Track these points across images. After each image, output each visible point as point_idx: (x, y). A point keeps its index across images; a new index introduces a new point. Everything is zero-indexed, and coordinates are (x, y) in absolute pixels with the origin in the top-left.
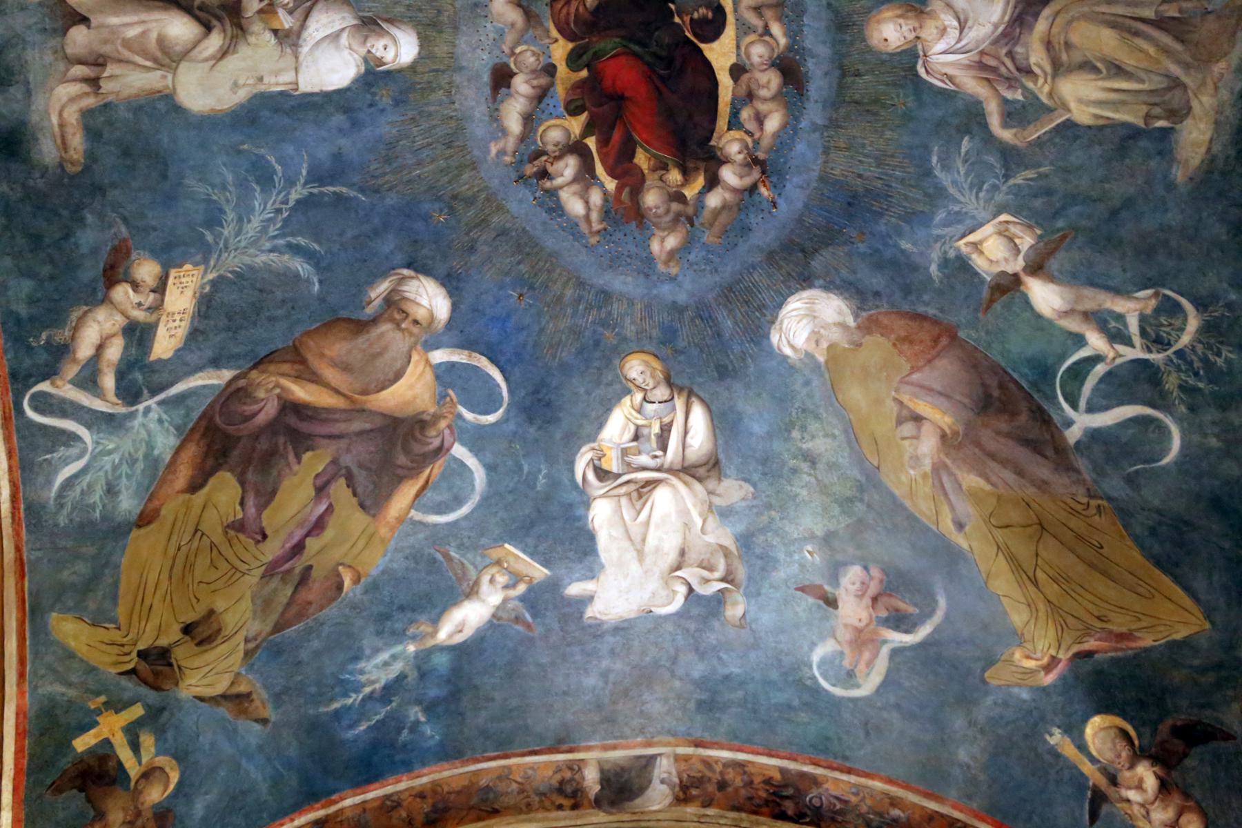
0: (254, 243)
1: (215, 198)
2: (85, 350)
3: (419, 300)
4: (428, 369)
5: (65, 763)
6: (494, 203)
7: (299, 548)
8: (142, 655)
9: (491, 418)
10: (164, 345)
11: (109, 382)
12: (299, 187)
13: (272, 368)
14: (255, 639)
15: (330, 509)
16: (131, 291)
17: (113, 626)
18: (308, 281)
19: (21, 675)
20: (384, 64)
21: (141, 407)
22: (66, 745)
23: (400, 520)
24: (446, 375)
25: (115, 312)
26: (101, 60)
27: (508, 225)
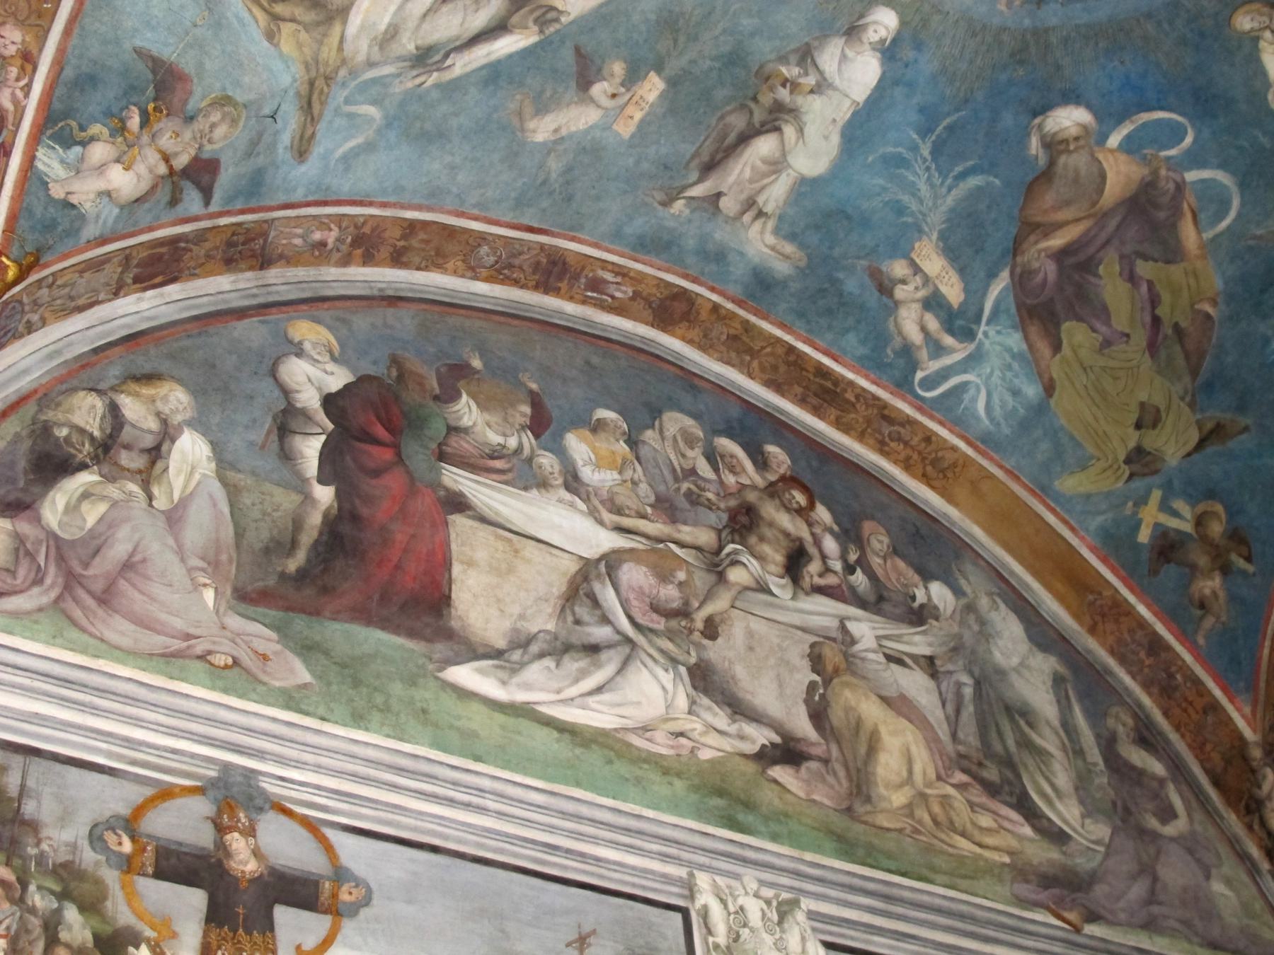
0: (936, 197)
1: (887, 199)
2: (915, 336)
3: (1063, 126)
4: (1118, 155)
5: (1145, 556)
6: (1040, 34)
7: (1156, 321)
8: (1128, 461)
9: (1189, 140)
10: (953, 292)
11: (948, 340)
12: (922, 146)
13: (1025, 246)
14: (1186, 392)
15: (1150, 284)
16: (905, 287)
18: (988, 184)
19: (1072, 529)
20: (886, 40)
21: (980, 335)
22: (1136, 547)
23: (1202, 246)
24: (1129, 147)
25: (909, 305)
26: (751, 202)
27: (1065, 33)
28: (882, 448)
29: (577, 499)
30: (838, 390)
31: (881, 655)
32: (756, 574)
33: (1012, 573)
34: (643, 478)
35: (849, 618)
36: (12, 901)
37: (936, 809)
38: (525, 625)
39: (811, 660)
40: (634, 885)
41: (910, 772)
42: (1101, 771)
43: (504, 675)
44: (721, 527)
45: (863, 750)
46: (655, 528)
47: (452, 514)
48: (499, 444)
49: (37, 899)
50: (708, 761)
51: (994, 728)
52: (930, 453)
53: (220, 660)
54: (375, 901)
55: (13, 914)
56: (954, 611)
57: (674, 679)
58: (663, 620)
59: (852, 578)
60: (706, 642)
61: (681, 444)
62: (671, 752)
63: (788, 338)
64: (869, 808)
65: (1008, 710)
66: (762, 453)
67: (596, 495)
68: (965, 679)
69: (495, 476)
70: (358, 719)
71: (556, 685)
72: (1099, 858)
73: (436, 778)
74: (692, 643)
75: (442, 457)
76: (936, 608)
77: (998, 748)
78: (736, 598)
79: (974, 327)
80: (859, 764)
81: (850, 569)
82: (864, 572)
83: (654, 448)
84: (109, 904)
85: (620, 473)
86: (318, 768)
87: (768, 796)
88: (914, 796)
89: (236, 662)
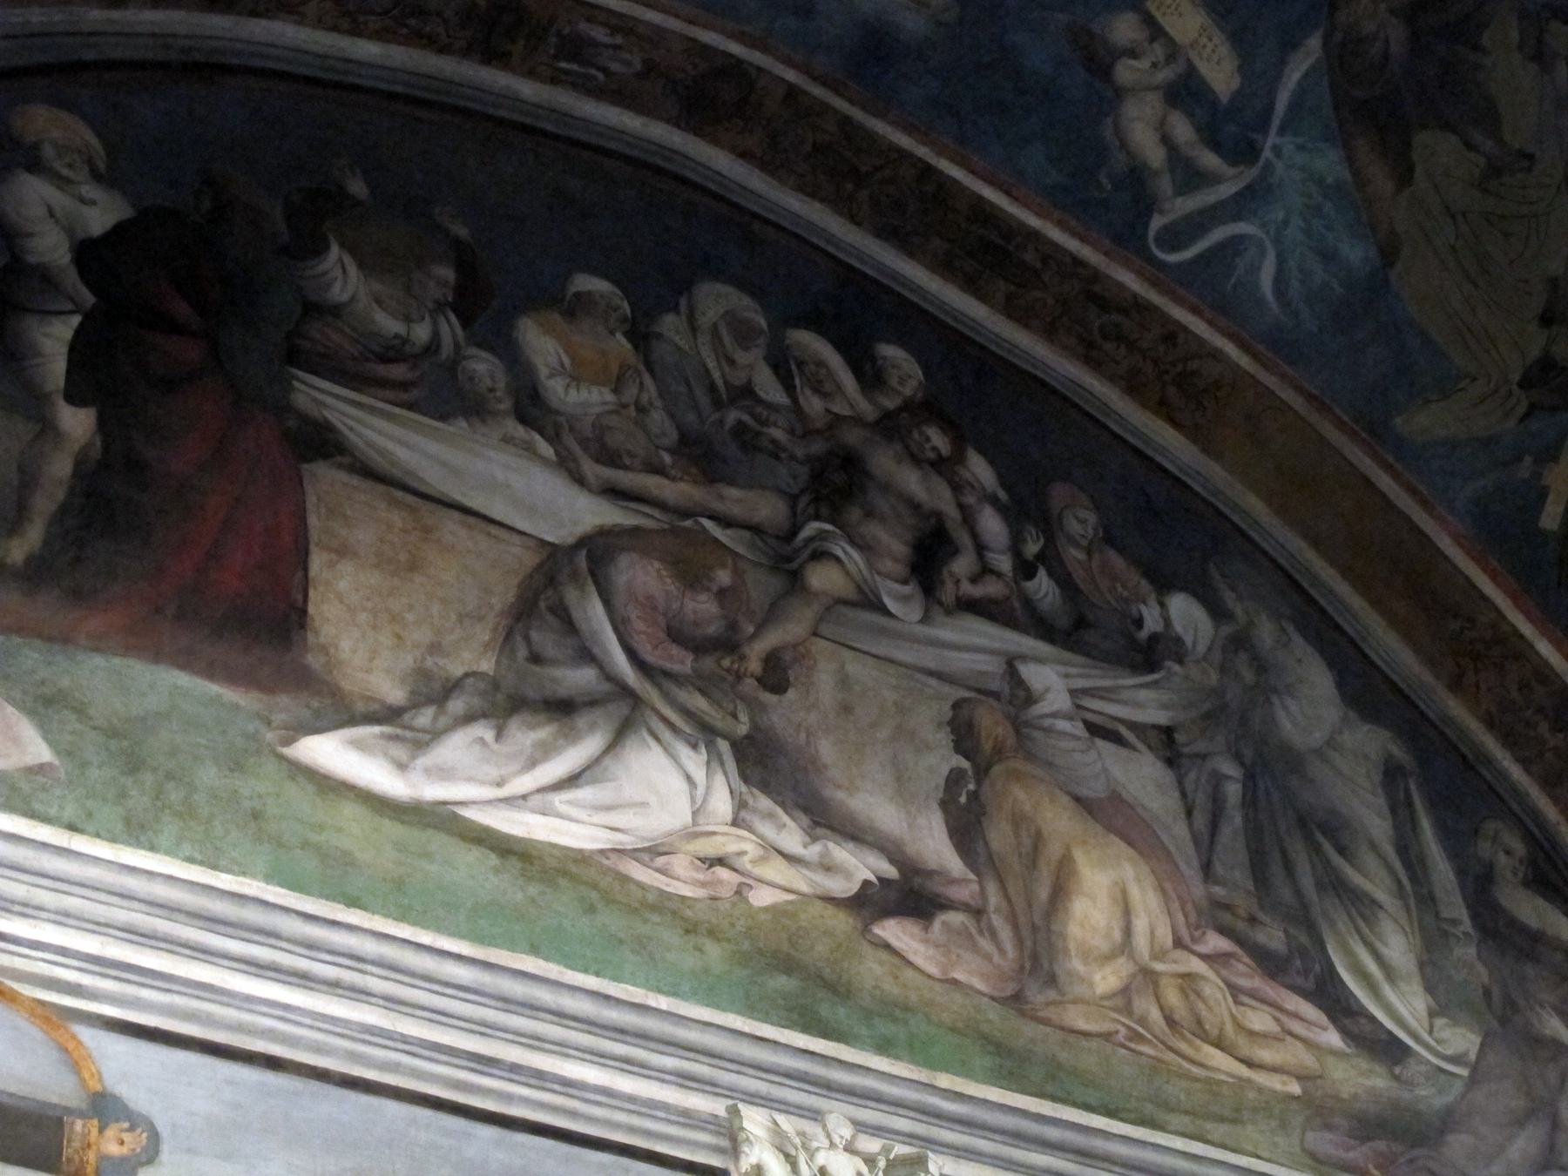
2: (1155, 155)
8: (1525, 383)
11: (1210, 160)
17: (1468, 380)
19: (1425, 504)
21: (1267, 153)
28: (1091, 357)
29: (537, 437)
30: (1011, 248)
31: (1081, 725)
32: (858, 578)
33: (1314, 578)
34: (658, 403)
35: (1024, 658)
37: (1173, 997)
38: (441, 662)
39: (952, 732)
40: (632, 1130)
41: (1128, 931)
42: (1465, 934)
43: (400, 752)
44: (795, 491)
45: (1043, 893)
46: (673, 490)
47: (310, 461)
48: (397, 336)
50: (766, 909)
51: (1276, 855)
52: (1173, 364)
54: (165, 1155)
56: (1210, 649)
57: (708, 763)
58: (689, 659)
59: (1030, 586)
60: (769, 698)
61: (727, 339)
62: (700, 893)
63: (923, 152)
64: (1052, 994)
65: (1303, 822)
66: (873, 359)
67: (572, 429)
68: (1229, 768)
69: (389, 394)
70: (136, 832)
71: (494, 772)
72: (1458, 1087)
73: (277, 936)
74: (742, 699)
75: (294, 356)
76: (1179, 640)
77: (1286, 893)
78: (821, 619)
79: (1259, 137)
80: (1037, 919)
81: (1026, 569)
82: (1050, 574)
83: (679, 348)
85: (615, 391)
86: (64, 918)
87: (871, 970)
88: (1134, 976)
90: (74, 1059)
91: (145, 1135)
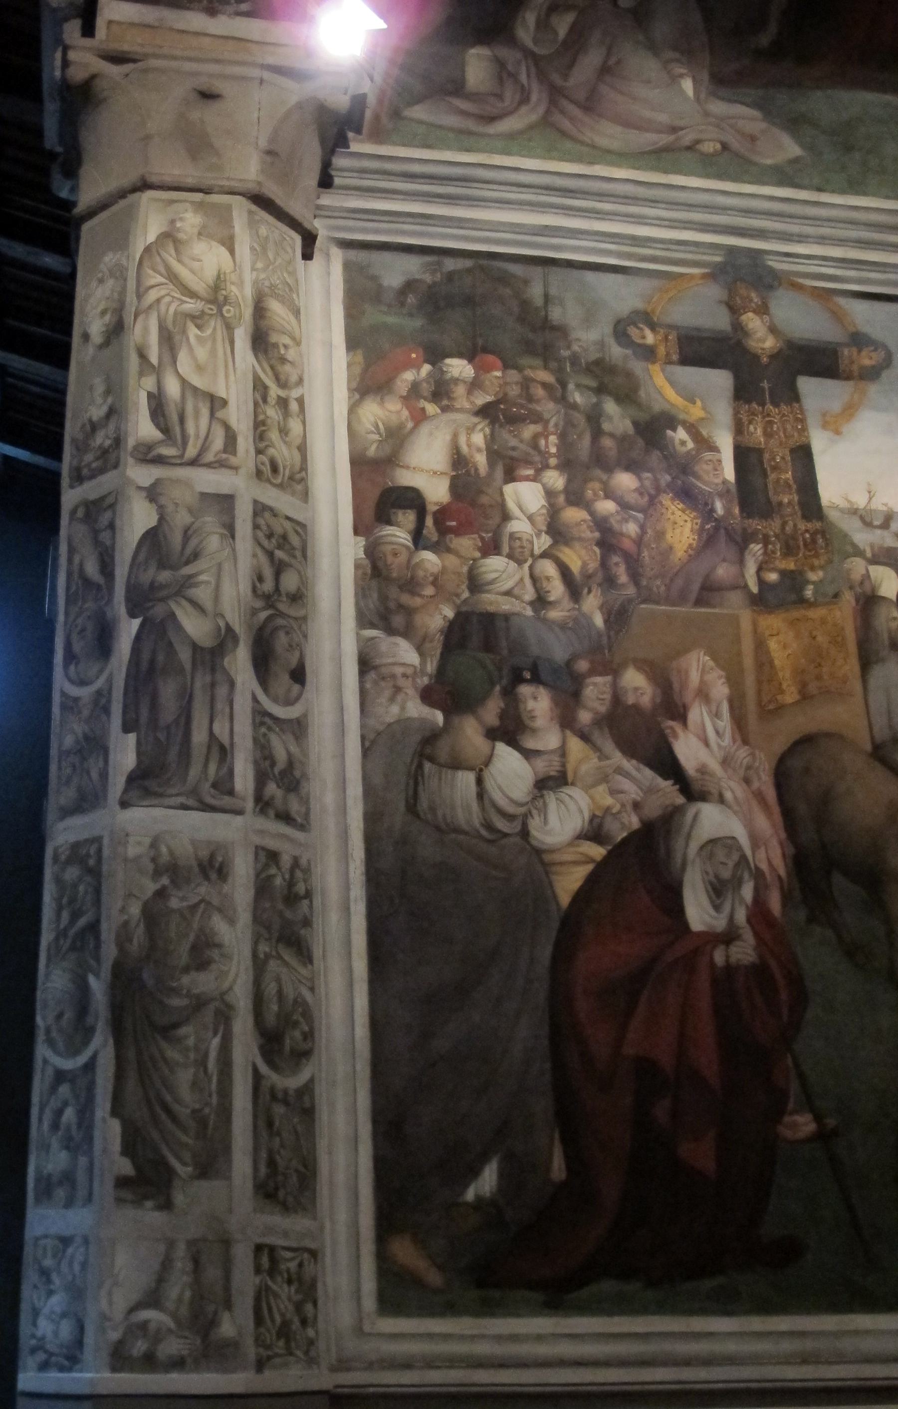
36: (556, 400)
49: (578, 397)
53: (709, 147)
55: (558, 412)
70: (854, 187)
84: (642, 393)
86: (822, 240)
89: (725, 147)
90: (838, 316)
91: (883, 352)
